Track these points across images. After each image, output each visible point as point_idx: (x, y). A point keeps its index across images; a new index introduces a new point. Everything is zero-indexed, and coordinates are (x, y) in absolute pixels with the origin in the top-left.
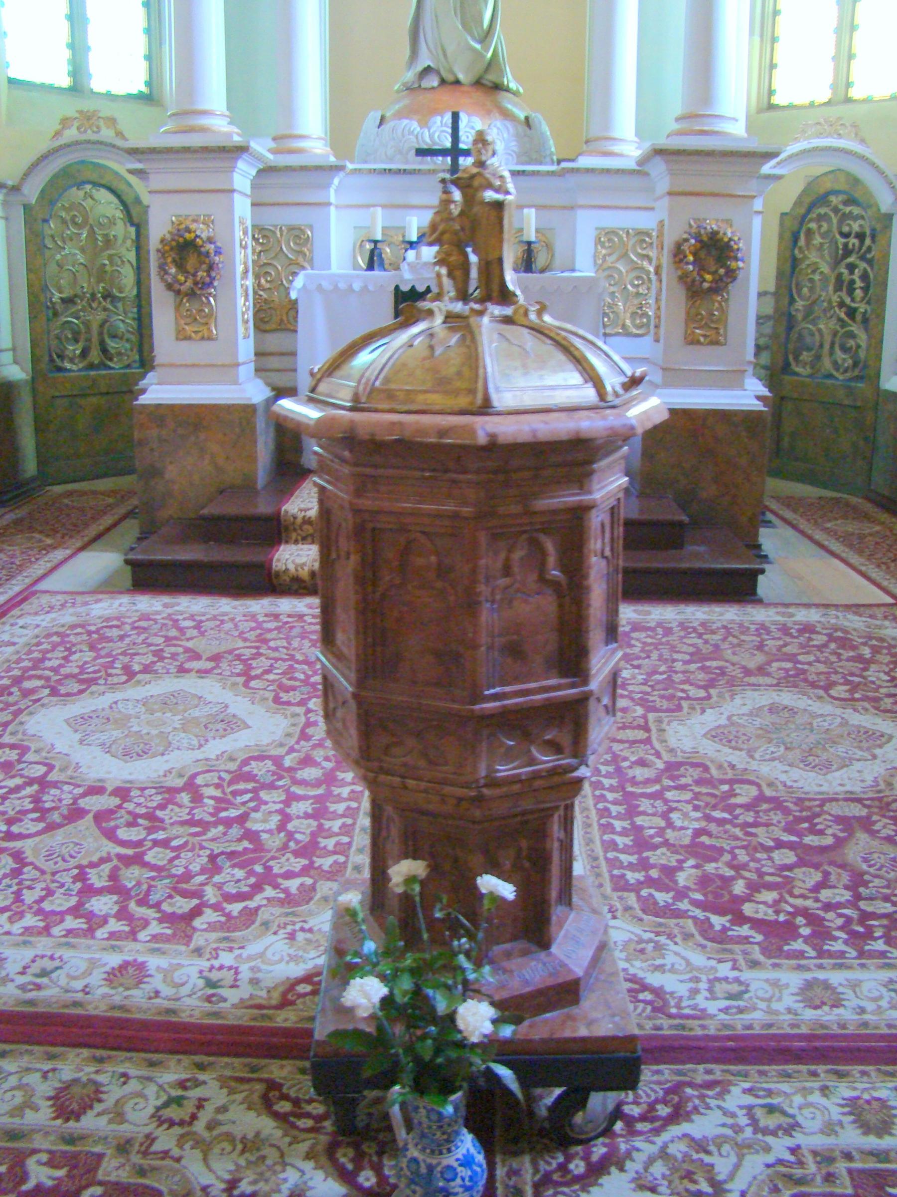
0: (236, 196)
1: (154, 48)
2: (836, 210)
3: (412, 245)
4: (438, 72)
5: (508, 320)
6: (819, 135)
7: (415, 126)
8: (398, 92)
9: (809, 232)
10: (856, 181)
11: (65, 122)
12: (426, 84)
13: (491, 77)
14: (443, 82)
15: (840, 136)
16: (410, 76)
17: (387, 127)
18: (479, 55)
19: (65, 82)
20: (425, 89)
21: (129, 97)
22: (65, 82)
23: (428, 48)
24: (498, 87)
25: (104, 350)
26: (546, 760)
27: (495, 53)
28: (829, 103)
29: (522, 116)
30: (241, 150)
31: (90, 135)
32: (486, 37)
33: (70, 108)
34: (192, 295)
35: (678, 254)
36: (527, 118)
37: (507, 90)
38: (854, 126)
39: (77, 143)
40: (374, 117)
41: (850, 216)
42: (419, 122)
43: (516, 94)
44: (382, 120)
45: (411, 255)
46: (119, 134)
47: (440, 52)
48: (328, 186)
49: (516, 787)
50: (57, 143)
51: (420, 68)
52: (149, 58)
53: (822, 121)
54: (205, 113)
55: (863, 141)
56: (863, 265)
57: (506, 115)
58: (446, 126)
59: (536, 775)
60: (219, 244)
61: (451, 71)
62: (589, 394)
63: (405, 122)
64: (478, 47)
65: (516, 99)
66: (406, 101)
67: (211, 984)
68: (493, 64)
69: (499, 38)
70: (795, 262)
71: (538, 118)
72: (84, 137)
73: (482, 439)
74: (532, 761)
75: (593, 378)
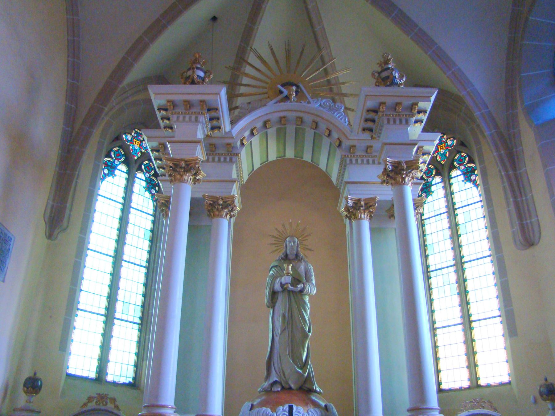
1: (139, 362)
4: (280, 383)
6: (473, 408)
7: (269, 410)
8: (260, 392)
11: (90, 399)
12: (275, 389)
13: (308, 386)
14: (283, 388)
15: (483, 408)
16: (266, 384)
17: (255, 411)
18: (301, 375)
19: (93, 375)
20: (275, 392)
21: (124, 384)
22: (93, 375)
23: (275, 370)
24: (311, 391)
27: (309, 373)
28: (469, 388)
29: (323, 404)
31: (103, 407)
32: (304, 366)
33: (94, 390)
36: (326, 406)
37: (315, 391)
38: (489, 402)
39: (94, 410)
40: (248, 405)
42: (272, 409)
43: (319, 393)
44: (252, 407)
46: (117, 407)
47: (282, 374)
50: (84, 409)
51: (271, 381)
52: (136, 366)
53: (473, 401)
54: (163, 406)
55: (495, 410)
57: (316, 405)
58: (285, 411)
61: (287, 382)
63: (264, 408)
64: (300, 371)
65: (319, 396)
66: (263, 398)
68: (308, 379)
69: (310, 365)
71: (331, 405)
72: (98, 407)
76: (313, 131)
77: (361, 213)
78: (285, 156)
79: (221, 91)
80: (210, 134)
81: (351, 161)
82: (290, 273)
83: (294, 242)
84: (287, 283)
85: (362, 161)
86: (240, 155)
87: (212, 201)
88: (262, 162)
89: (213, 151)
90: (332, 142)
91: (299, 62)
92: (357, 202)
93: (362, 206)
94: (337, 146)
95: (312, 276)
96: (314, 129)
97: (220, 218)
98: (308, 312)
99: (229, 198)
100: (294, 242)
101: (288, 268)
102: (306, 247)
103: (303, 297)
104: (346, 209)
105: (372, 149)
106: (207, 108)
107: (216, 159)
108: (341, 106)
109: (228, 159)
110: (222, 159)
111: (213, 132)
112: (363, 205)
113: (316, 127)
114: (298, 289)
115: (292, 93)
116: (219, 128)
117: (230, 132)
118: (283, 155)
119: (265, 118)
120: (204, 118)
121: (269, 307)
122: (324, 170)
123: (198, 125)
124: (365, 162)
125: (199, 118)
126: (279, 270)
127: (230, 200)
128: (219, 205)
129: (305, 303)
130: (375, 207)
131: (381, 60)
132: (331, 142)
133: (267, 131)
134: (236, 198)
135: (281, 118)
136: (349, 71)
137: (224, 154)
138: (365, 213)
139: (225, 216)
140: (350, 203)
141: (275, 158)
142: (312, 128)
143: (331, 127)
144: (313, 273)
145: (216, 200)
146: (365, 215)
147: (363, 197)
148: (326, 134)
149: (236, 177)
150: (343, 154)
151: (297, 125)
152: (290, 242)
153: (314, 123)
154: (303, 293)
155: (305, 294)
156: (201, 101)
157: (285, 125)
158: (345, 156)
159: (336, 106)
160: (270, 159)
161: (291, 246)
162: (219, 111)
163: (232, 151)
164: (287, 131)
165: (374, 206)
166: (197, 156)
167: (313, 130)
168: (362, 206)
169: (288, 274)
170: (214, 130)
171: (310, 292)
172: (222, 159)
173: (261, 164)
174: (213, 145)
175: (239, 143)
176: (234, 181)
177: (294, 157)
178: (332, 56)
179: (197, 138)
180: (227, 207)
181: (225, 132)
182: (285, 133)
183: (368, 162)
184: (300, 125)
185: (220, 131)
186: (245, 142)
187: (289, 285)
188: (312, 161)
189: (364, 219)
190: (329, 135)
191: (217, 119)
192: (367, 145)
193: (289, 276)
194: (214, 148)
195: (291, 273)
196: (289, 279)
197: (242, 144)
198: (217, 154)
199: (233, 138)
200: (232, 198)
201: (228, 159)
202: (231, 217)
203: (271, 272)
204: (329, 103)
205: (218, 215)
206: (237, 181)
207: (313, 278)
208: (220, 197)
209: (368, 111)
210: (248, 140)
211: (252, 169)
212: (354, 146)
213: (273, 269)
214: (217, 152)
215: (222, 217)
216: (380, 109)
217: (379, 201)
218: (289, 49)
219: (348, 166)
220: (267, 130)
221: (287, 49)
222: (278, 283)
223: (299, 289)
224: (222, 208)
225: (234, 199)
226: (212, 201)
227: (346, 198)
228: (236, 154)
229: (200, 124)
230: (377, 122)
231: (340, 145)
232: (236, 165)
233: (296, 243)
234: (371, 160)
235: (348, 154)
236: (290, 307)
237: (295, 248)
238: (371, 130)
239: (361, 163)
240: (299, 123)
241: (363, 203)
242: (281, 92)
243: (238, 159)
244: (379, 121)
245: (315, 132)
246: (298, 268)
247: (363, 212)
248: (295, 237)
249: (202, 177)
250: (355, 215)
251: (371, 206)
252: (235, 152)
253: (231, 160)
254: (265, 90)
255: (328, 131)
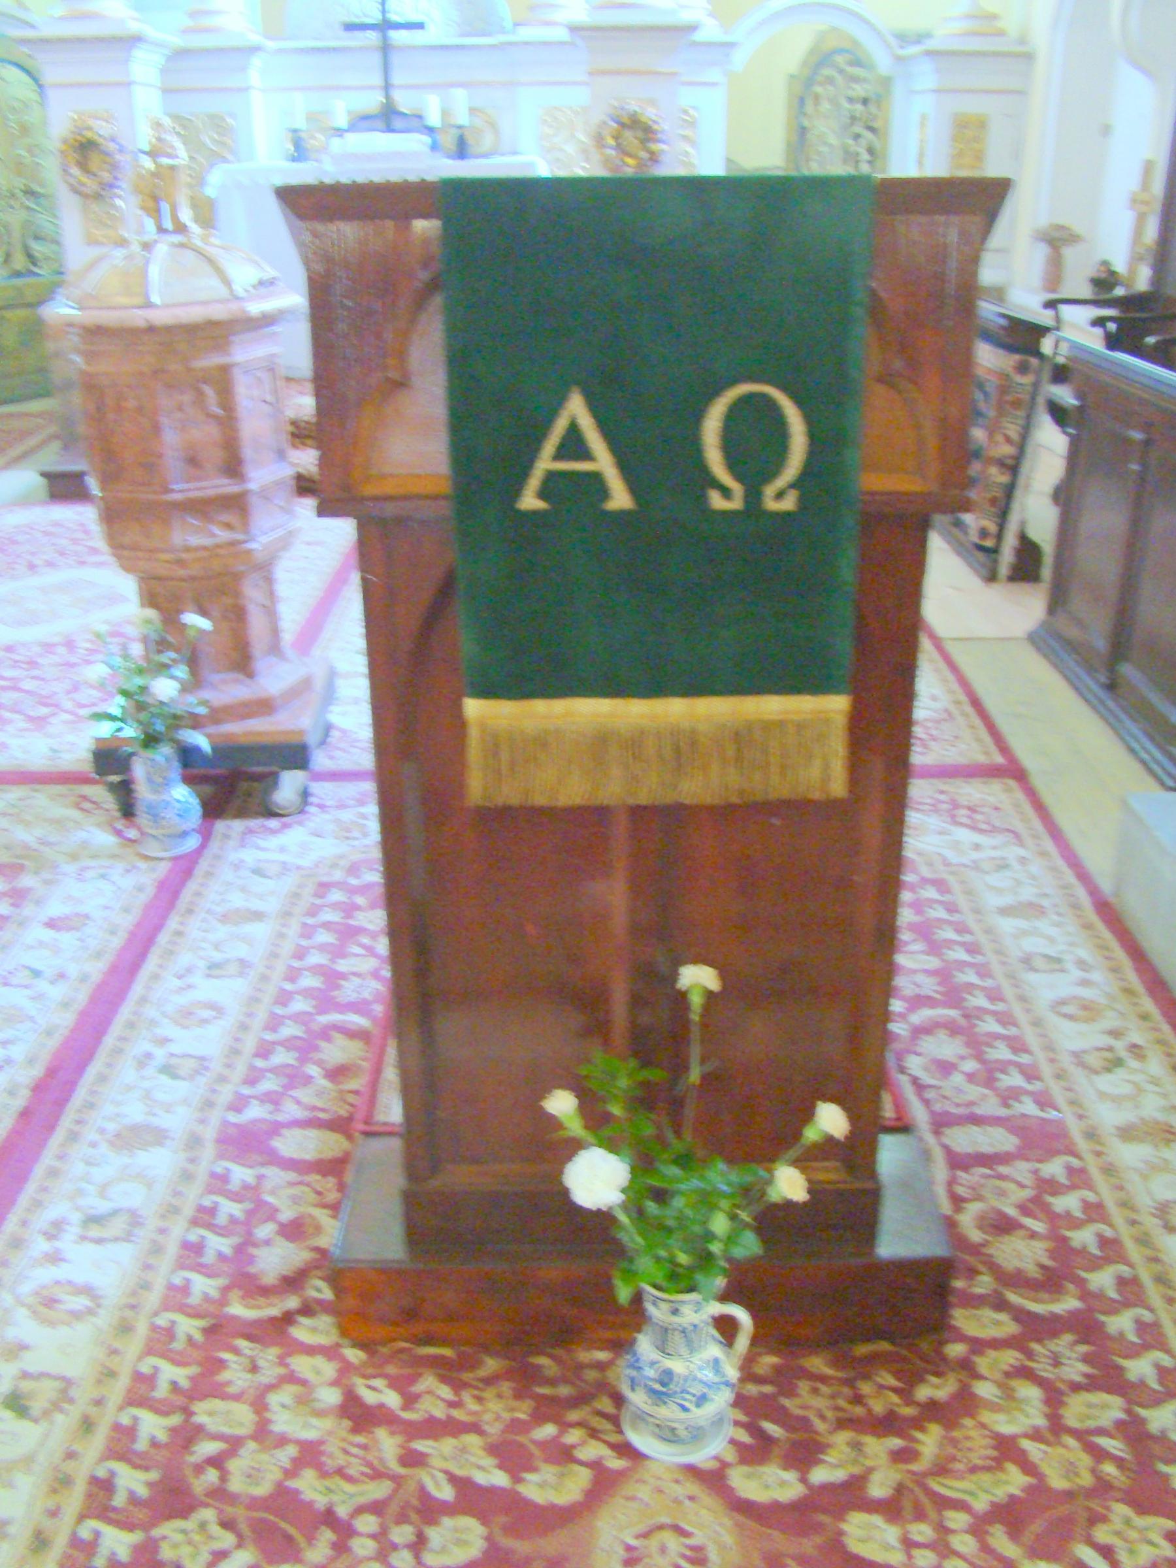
0: (137, 91)
2: (841, 71)
3: (339, 132)
5: (182, 246)
9: (817, 98)
10: (855, 43)
25: (30, 256)
26: (223, 535)
30: (136, 40)
34: (98, 197)
35: (599, 140)
41: (855, 79)
45: (336, 144)
48: (243, 69)
49: (205, 554)
56: (868, 135)
59: (218, 546)
60: (123, 142)
62: (223, 292)
67: (55, 751)
70: (803, 131)
73: (142, 324)
74: (214, 535)
75: (227, 283)
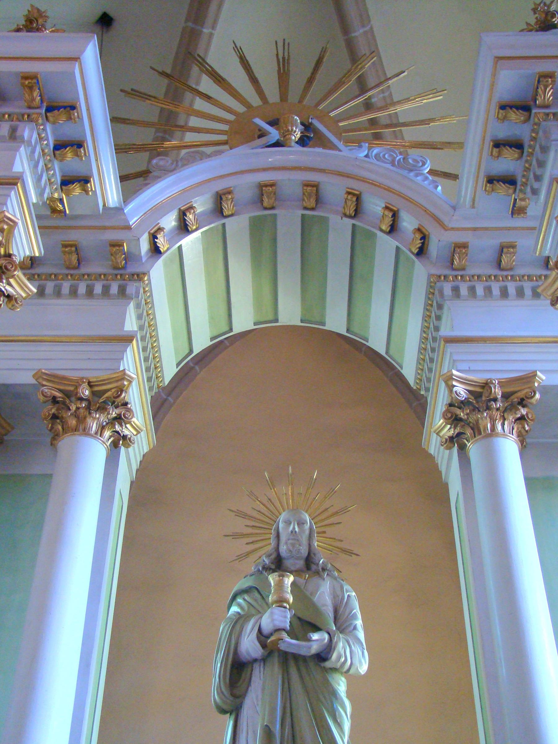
76: (349, 222)
77: (493, 421)
78: (276, 320)
79: (83, 52)
80: (61, 201)
81: (456, 290)
82: (288, 602)
83: (301, 523)
84: (278, 630)
85: (488, 290)
86: (149, 279)
87: (60, 391)
88: (215, 334)
89: (75, 268)
90: (400, 246)
91: (311, 81)
92: (478, 390)
93: (495, 400)
94: (416, 251)
95: (354, 617)
96: (350, 217)
97: (81, 435)
98: (347, 725)
99: (109, 381)
100: (301, 523)
101: (280, 585)
102: (339, 544)
103: (330, 679)
104: (449, 415)
105: (514, 253)
106: (45, 104)
107: (82, 289)
108: (421, 160)
109: (114, 289)
110: (98, 288)
111: (67, 196)
112: (499, 397)
113: (356, 211)
114: (310, 647)
115: (290, 128)
116: (85, 181)
117: (119, 210)
118: (271, 317)
119: (220, 186)
120: (35, 136)
121: (223, 711)
122: (382, 352)
123: (17, 149)
124: (496, 291)
125: (19, 129)
126: (256, 600)
127: (111, 389)
128: (81, 399)
129: (334, 693)
130: (533, 401)
131: (529, 22)
132: (398, 249)
133: (224, 225)
134: (130, 382)
135: (262, 187)
136: (441, 97)
137: (102, 276)
138: (504, 419)
139: (96, 433)
140: (461, 390)
141: (250, 326)
142: (345, 215)
143: (397, 203)
144: (357, 611)
145: (72, 388)
146: (506, 426)
147: (496, 377)
148: (384, 228)
149: (135, 329)
150: (434, 271)
151: (306, 208)
152: (288, 523)
153: (349, 197)
154: (328, 664)
155: (335, 670)
156: (26, 77)
157: (273, 208)
158: (440, 277)
159: (410, 161)
160: (238, 328)
161: (293, 532)
162: (80, 117)
163: (124, 268)
164: (281, 230)
165: (532, 397)
166: (3, 212)
167: (346, 220)
168: (495, 400)
169: (281, 602)
170: (71, 187)
171: (351, 664)
172: (98, 288)
173: (212, 339)
174: (71, 246)
175: (144, 246)
176: (128, 339)
177: (302, 321)
178: (392, 99)
179: (13, 171)
180: (102, 409)
181: (104, 205)
182: (274, 240)
183: (504, 294)
184: (313, 209)
185: (87, 192)
186: (161, 241)
187: (285, 635)
188: (348, 331)
189: (504, 436)
190: (393, 229)
191: (75, 147)
192: (500, 241)
193: (285, 607)
194: (74, 258)
195: (291, 600)
196: (286, 617)
197: (156, 251)
198: (84, 275)
199: (128, 228)
200: (117, 381)
201: (114, 289)
202: (115, 445)
203: (234, 609)
204: (390, 155)
205: (76, 429)
206: (137, 341)
207: (359, 623)
208: (83, 378)
209: (503, 107)
210: (172, 241)
211: (187, 351)
212: (465, 246)
213: (240, 600)
214: (83, 270)
215: (86, 432)
216: (538, 97)
217: (545, 390)
218: (286, 57)
219: (447, 305)
220: (224, 221)
221: (281, 56)
222: (251, 632)
223: (315, 648)
224: (88, 408)
225: (126, 383)
226: (60, 391)
227: (448, 379)
228: (138, 275)
229: (22, 149)
230: (530, 146)
231: (421, 252)
232: (138, 306)
233: (307, 526)
234: (512, 288)
235: (448, 272)
236: (288, 705)
237: (304, 540)
238: (510, 181)
239: (485, 296)
240: (312, 203)
241: (498, 392)
242: (262, 134)
243: (142, 291)
244: (534, 139)
245: (354, 225)
246: (313, 594)
247: (499, 416)
248: (306, 512)
249: (24, 295)
250: (476, 430)
251: (522, 403)
252: (131, 269)
253: (122, 291)
254: (224, 138)
255: (390, 215)
